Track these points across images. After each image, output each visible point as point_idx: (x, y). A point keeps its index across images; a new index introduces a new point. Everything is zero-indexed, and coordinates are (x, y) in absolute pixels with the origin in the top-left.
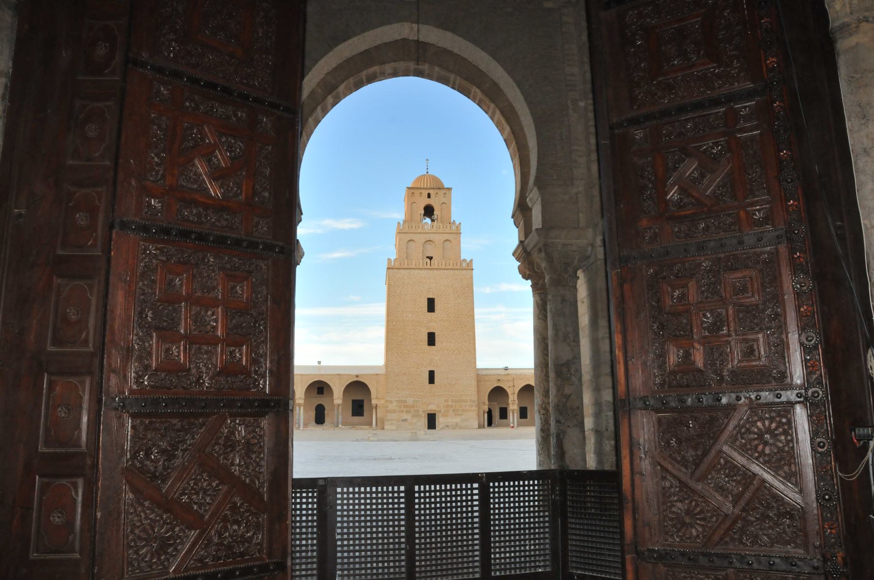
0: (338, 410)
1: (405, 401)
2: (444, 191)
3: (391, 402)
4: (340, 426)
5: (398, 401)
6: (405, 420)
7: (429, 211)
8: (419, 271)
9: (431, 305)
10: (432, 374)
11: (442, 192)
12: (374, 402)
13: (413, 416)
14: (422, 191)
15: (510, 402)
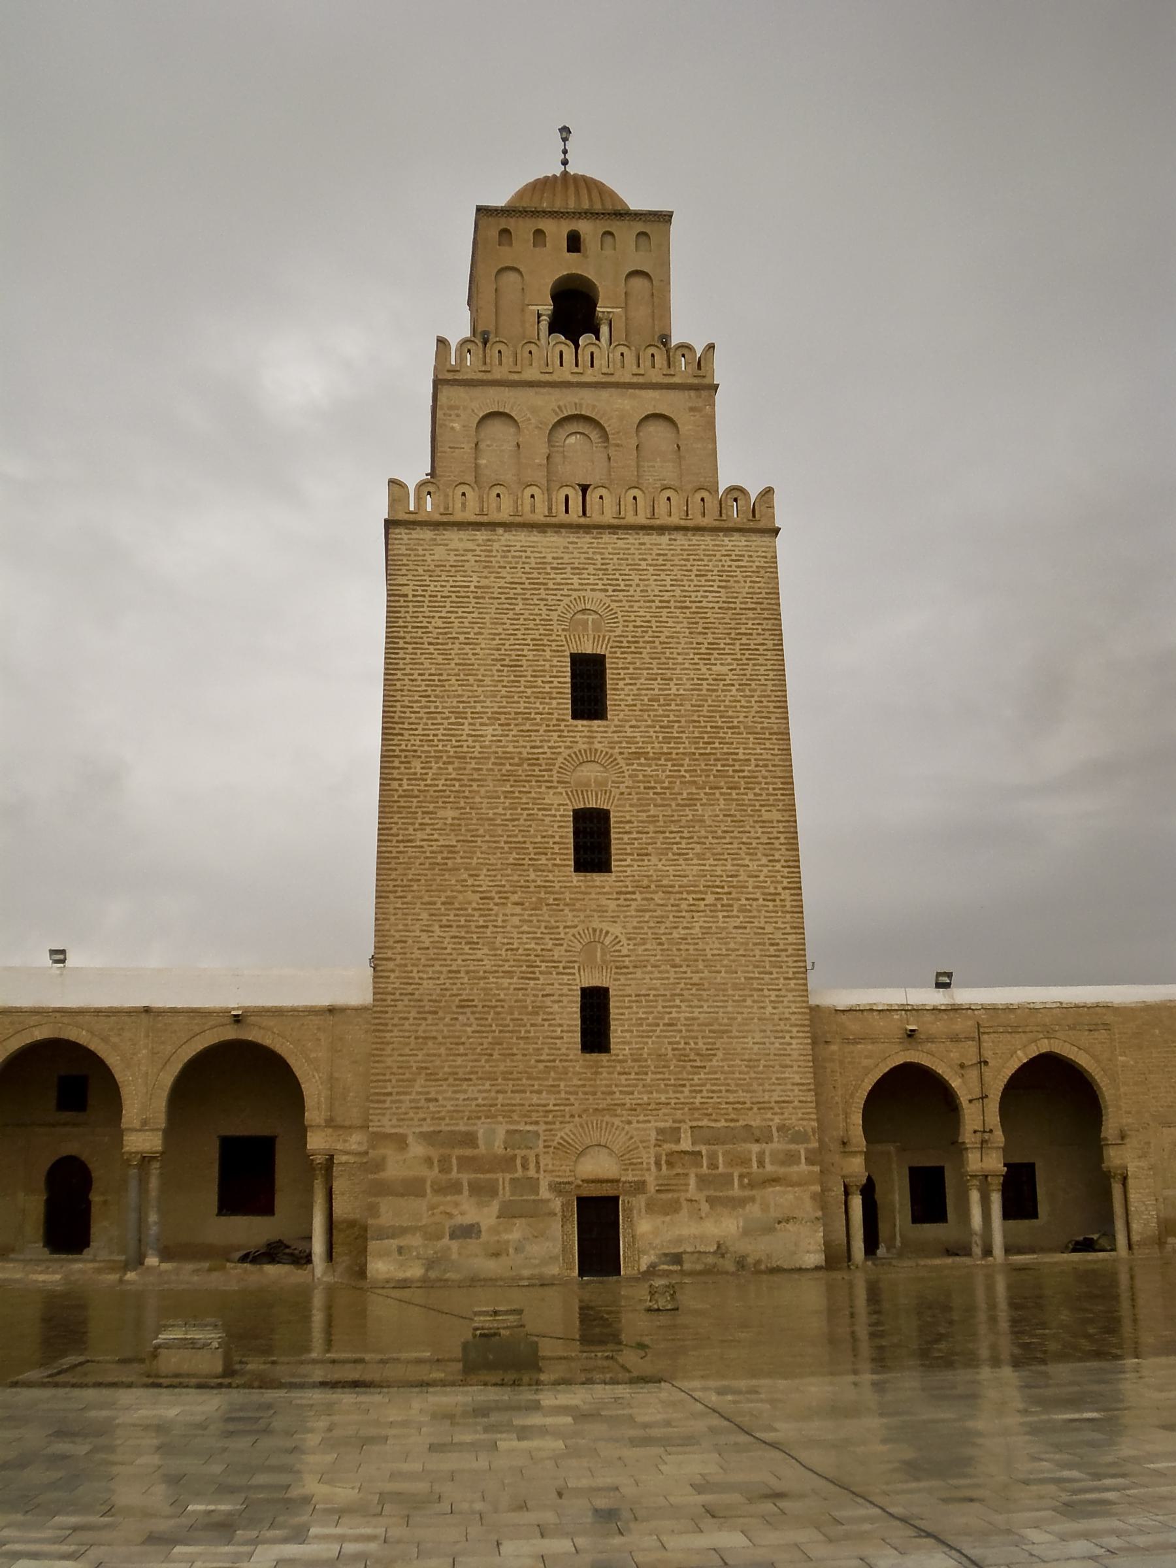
0: (143, 1181)
1: (470, 1139)
2: (640, 227)
3: (401, 1142)
4: (152, 1261)
5: (429, 1138)
6: (468, 1232)
7: (574, 311)
8: (536, 537)
9: (589, 687)
10: (595, 1008)
11: (626, 233)
12: (316, 1142)
13: (508, 1213)
14: (547, 225)
15: (968, 1136)
